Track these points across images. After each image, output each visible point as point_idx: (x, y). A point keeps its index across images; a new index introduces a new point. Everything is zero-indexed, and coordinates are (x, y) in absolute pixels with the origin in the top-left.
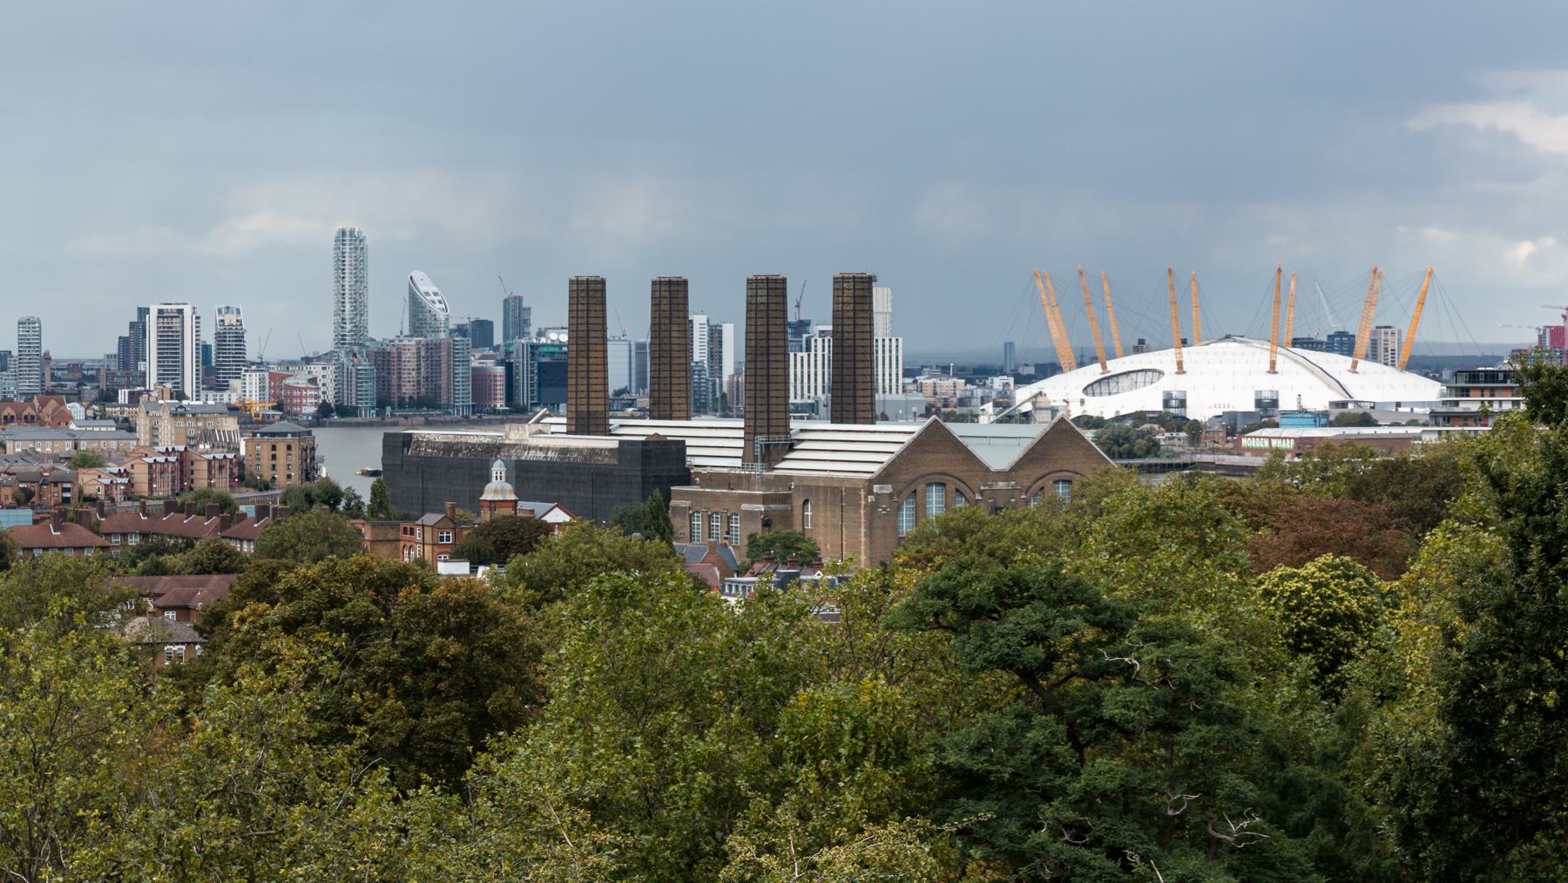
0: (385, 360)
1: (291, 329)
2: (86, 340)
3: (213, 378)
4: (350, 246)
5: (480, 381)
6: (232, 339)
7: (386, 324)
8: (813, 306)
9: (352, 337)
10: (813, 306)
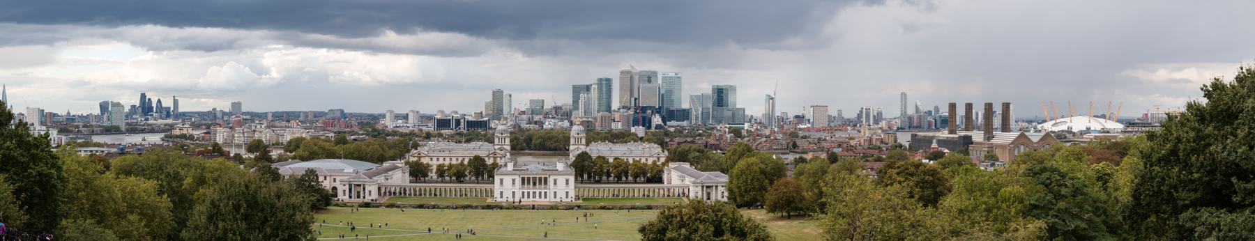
0: (910, 119)
1: (893, 112)
2: (851, 114)
3: (876, 122)
4: (904, 95)
5: (930, 123)
6: (880, 114)
7: (911, 111)
8: (998, 109)
9: (904, 114)
10: (998, 109)
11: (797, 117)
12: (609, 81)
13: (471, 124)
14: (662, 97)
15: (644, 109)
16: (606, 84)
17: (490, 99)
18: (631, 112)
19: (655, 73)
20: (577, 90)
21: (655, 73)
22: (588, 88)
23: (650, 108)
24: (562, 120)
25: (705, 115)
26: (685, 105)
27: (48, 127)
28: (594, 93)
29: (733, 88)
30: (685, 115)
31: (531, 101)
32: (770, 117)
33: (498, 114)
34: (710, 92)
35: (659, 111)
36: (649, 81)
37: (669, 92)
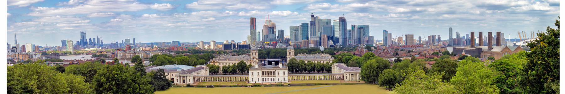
0: (454, 40)
5: (463, 42)
6: (439, 38)
7: (454, 36)
8: (494, 35)
10: (494, 35)
12: (307, 24)
13: (241, 47)
21: (330, 20)
27: (206, 63)
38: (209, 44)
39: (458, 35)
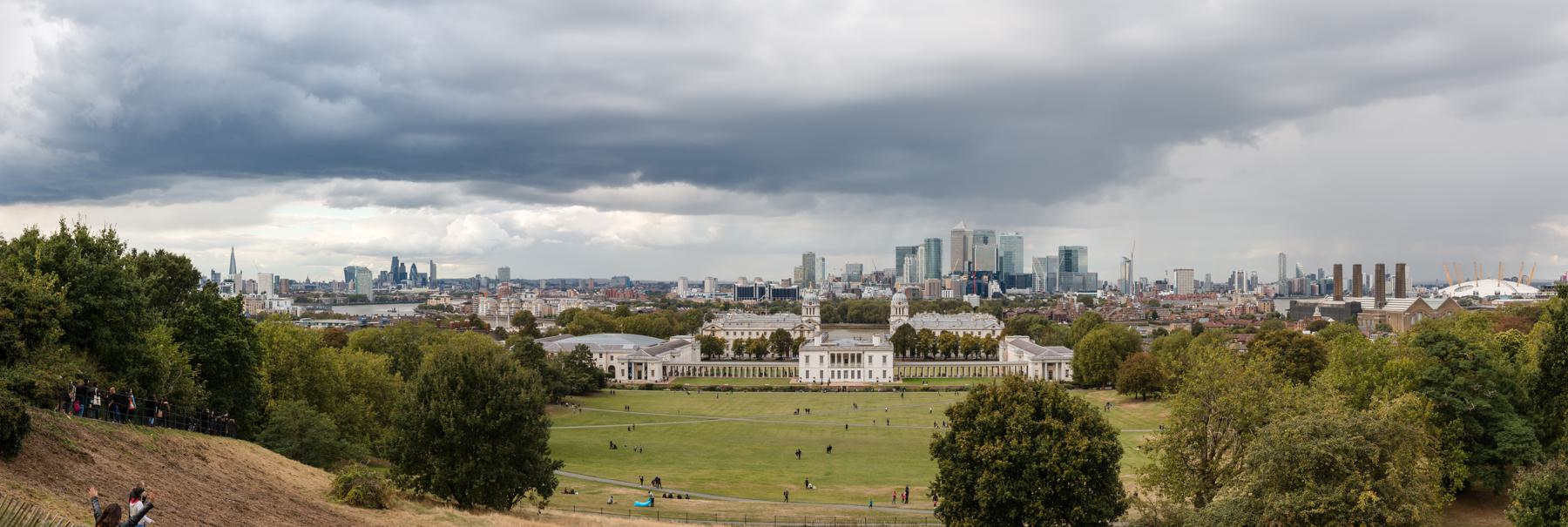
0: (1290, 283)
1: (1269, 277)
2: (1223, 280)
3: (1250, 288)
5: (1313, 288)
6: (1254, 279)
7: (1291, 275)
8: (1391, 271)
9: (1283, 278)
10: (1391, 271)
11: (1158, 282)
12: (938, 241)
13: (777, 293)
14: (1000, 261)
15: (979, 275)
16: (935, 246)
17: (799, 262)
18: (964, 278)
19: (992, 232)
20: (902, 253)
21: (992, 232)
22: (914, 251)
23: (986, 273)
24: (884, 287)
25: (1051, 281)
26: (1028, 270)
28: (921, 256)
29: (1084, 250)
30: (1027, 281)
31: (848, 266)
32: (1127, 283)
33: (809, 279)
34: (1056, 254)
35: (996, 277)
36: (986, 241)
37: (1009, 254)
38: (702, 286)
39: (1298, 273)
